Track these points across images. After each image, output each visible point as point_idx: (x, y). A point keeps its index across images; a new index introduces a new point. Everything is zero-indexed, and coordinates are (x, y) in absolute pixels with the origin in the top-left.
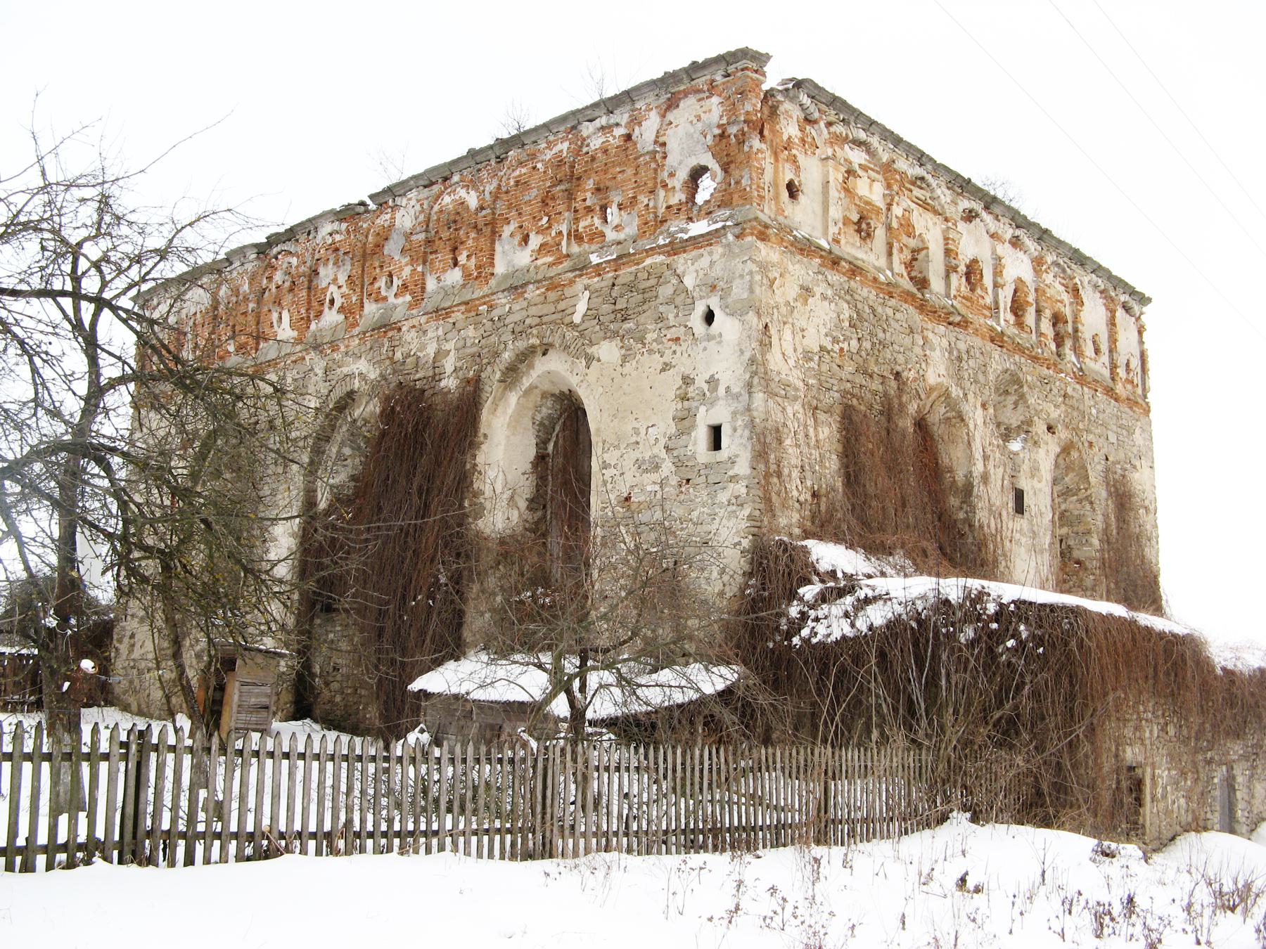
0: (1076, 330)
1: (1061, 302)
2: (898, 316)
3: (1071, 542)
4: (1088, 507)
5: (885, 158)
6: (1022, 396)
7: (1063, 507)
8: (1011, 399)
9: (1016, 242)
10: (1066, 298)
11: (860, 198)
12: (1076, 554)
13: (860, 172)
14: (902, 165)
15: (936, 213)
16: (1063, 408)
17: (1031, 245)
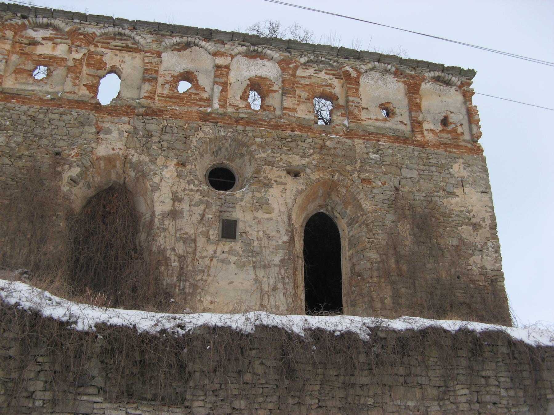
0: (347, 101)
1: (331, 86)
2: (64, 117)
3: (354, 260)
4: (365, 229)
5: (67, 29)
6: (251, 153)
7: (351, 233)
8: (247, 158)
9: (254, 55)
10: (336, 82)
11: (40, 56)
12: (357, 268)
13: (43, 42)
14: (91, 29)
15: (140, 51)
16: (316, 157)
17: (276, 55)
